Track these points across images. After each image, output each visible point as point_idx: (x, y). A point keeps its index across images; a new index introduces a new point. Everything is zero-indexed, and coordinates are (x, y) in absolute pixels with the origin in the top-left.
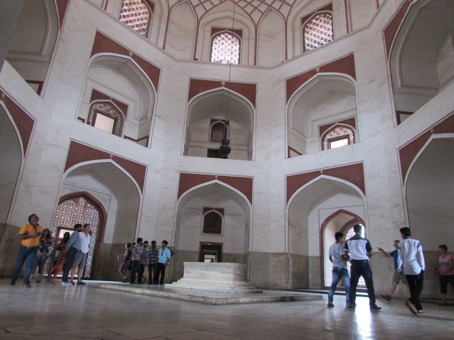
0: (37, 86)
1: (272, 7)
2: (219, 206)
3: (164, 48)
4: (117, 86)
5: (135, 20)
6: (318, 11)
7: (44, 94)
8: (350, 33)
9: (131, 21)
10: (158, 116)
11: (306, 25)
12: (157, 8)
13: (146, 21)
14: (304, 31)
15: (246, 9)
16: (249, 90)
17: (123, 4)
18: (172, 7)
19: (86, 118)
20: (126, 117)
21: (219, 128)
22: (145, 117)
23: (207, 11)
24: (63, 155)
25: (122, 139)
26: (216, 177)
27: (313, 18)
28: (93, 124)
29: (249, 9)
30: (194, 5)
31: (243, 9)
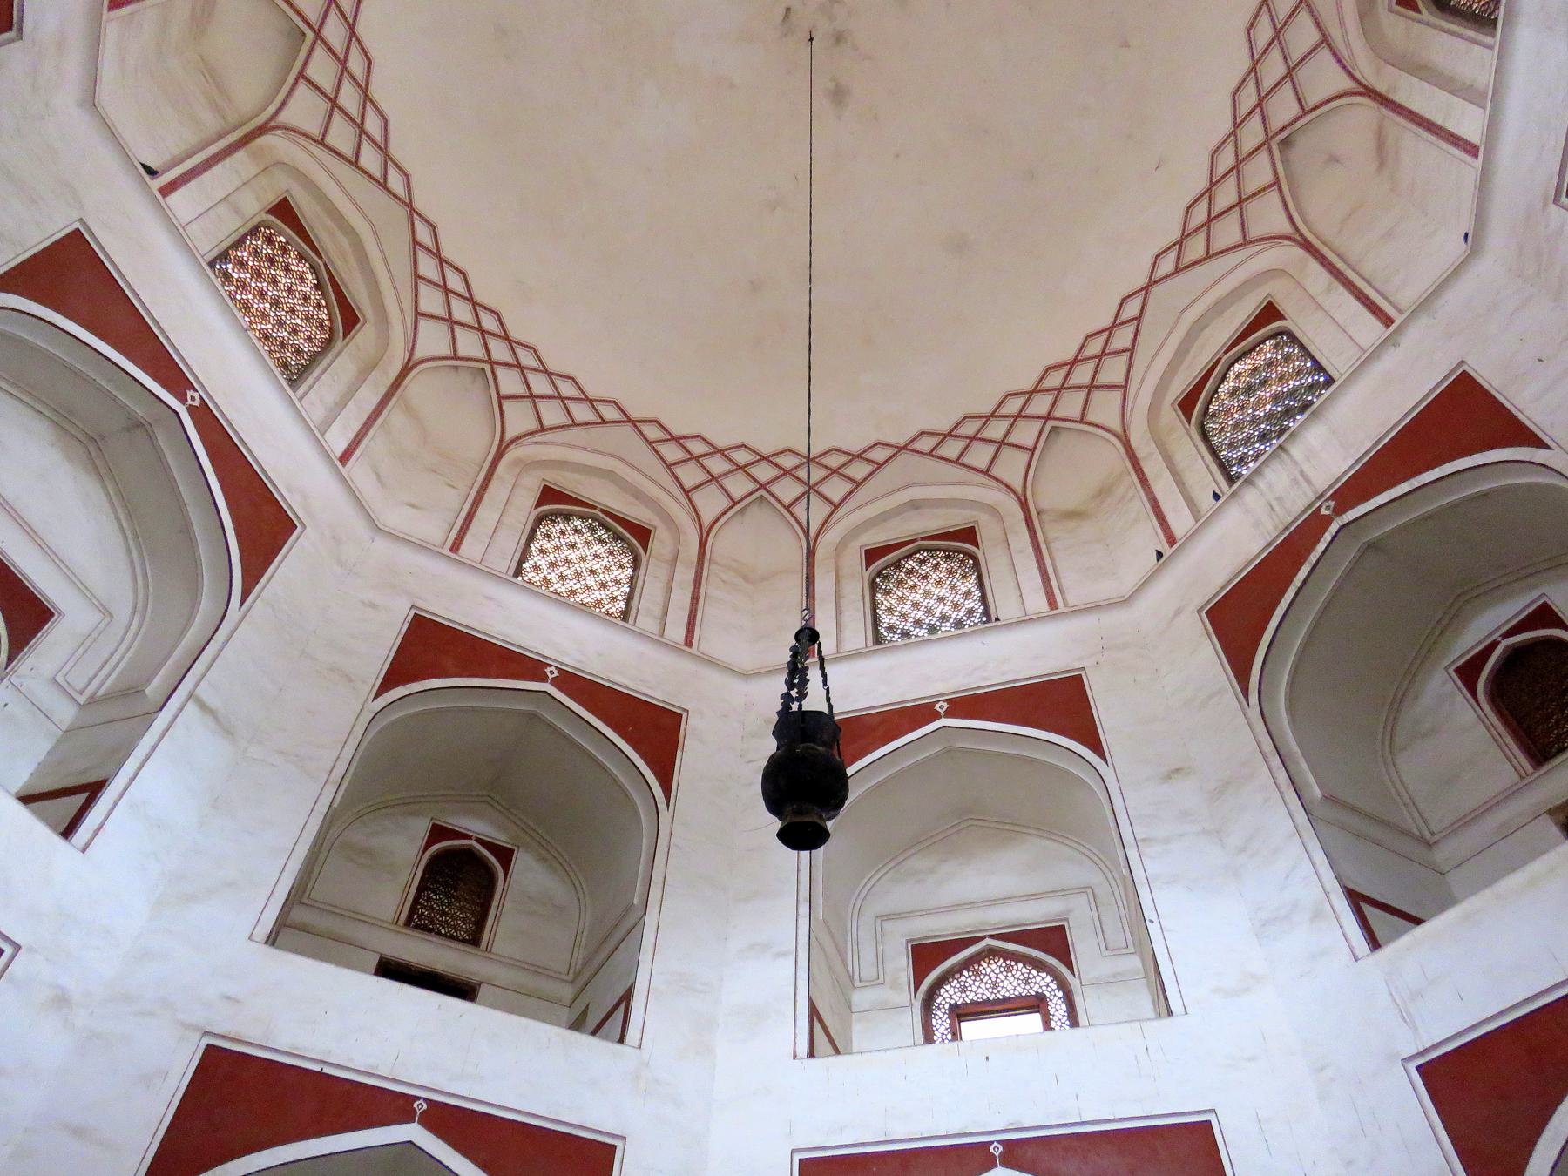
3: (689, 641)
15: (966, 460)
16: (1060, 705)
26: (996, 1150)
29: (980, 456)
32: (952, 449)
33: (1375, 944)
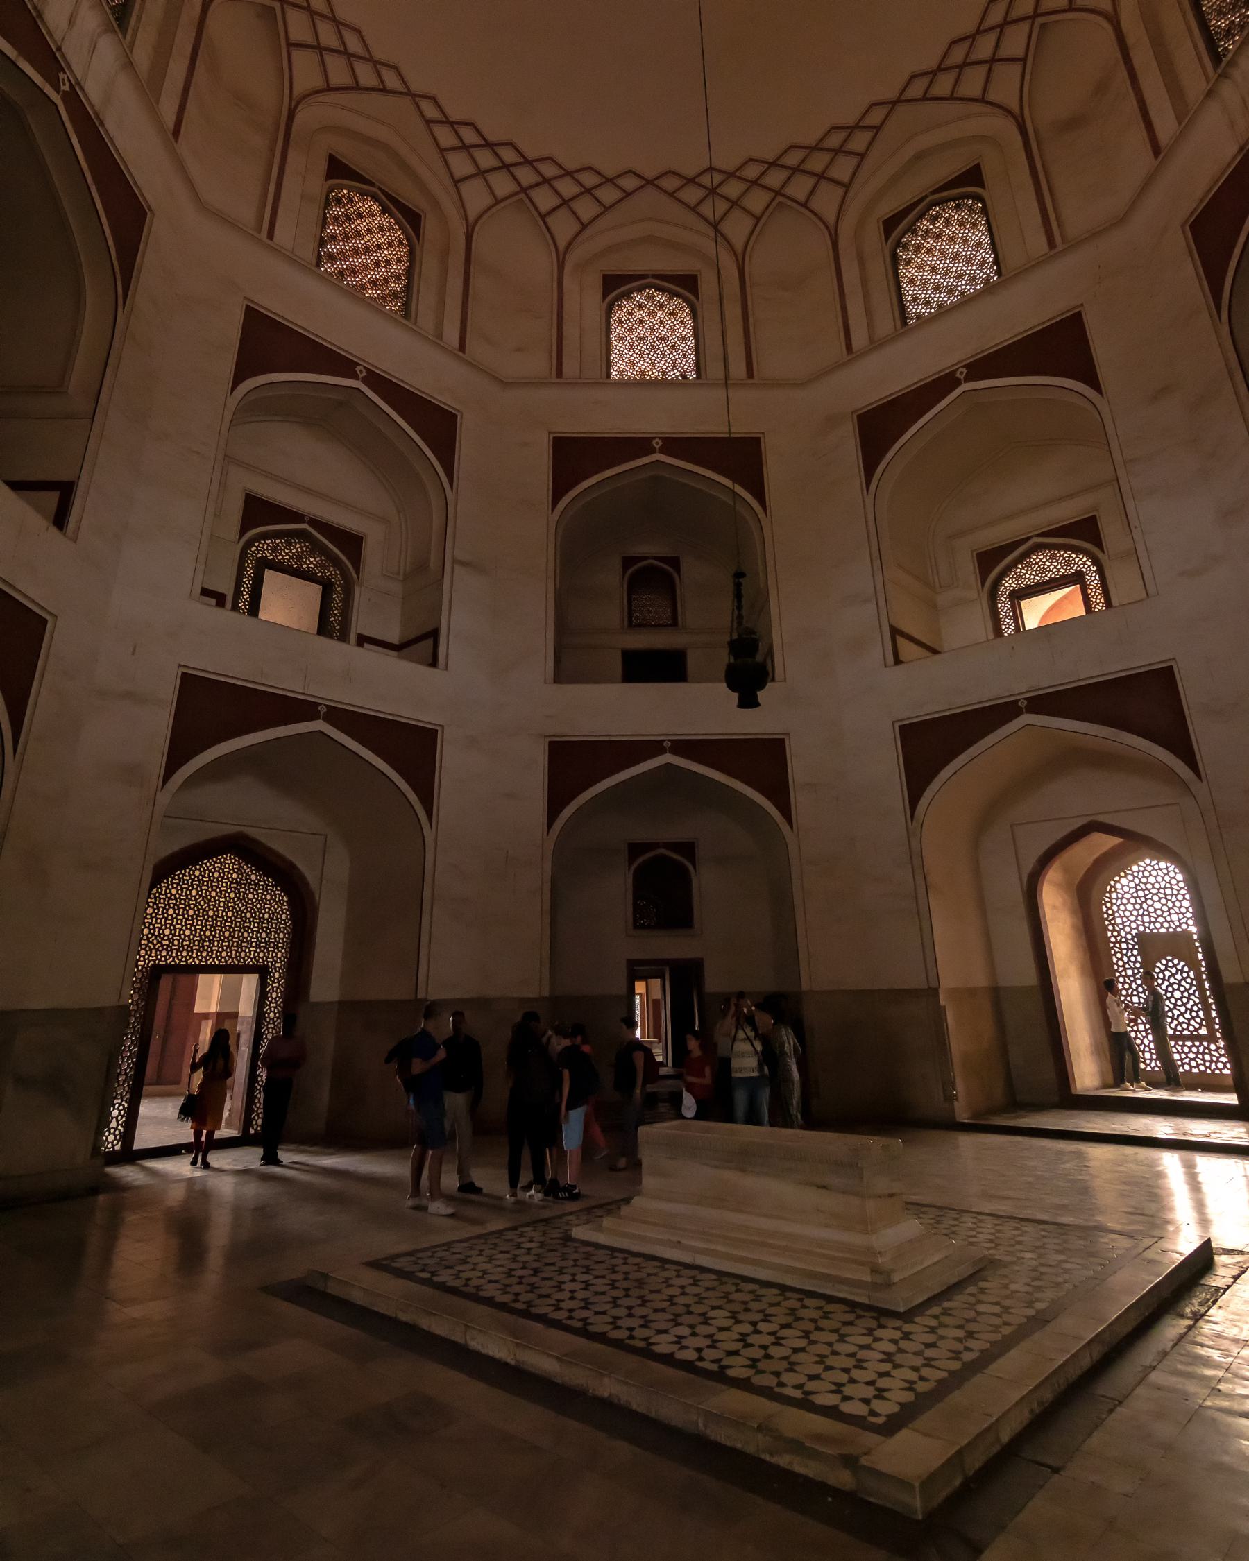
0: (53, 498)
1: (783, 195)
2: (679, 833)
3: (462, 347)
4: (321, 477)
5: (366, 268)
6: (934, 192)
7: (79, 522)
8: (1060, 247)
9: (353, 271)
10: (463, 564)
12: (430, 226)
14: (895, 259)
17: (325, 218)
18: (476, 221)
19: (227, 588)
20: (358, 574)
21: (652, 581)
22: (421, 566)
23: (584, 227)
24: (160, 722)
25: (349, 649)
27: (921, 217)
28: (254, 610)
30: (543, 209)
31: (693, 209)
32: (692, 195)
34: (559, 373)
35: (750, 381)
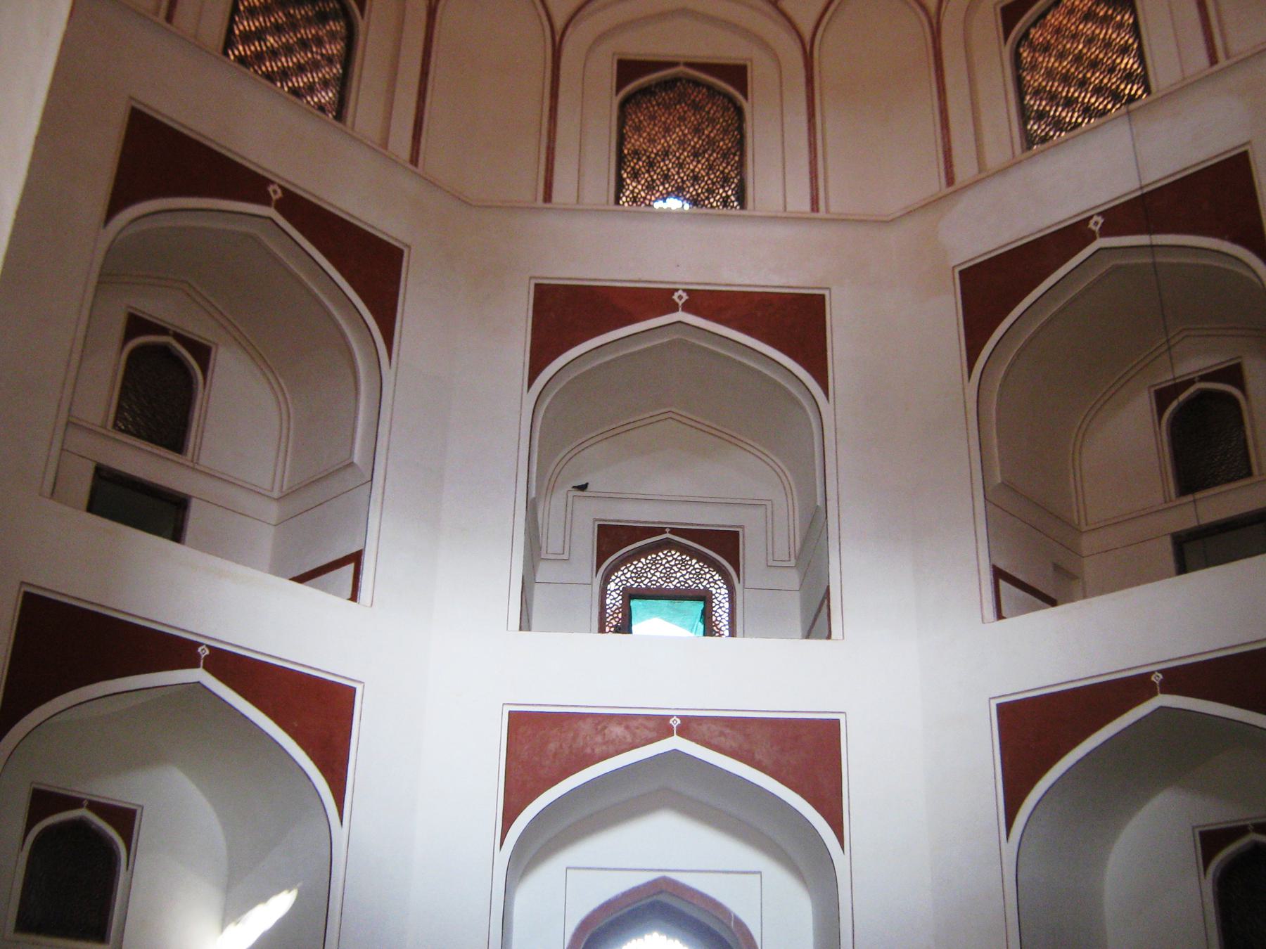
3: (414, 160)
8: (1223, 62)
11: (1026, 35)
13: (334, 49)
16: (796, 323)
26: (675, 723)
33: (1000, 616)
34: (548, 197)
35: (815, 215)
